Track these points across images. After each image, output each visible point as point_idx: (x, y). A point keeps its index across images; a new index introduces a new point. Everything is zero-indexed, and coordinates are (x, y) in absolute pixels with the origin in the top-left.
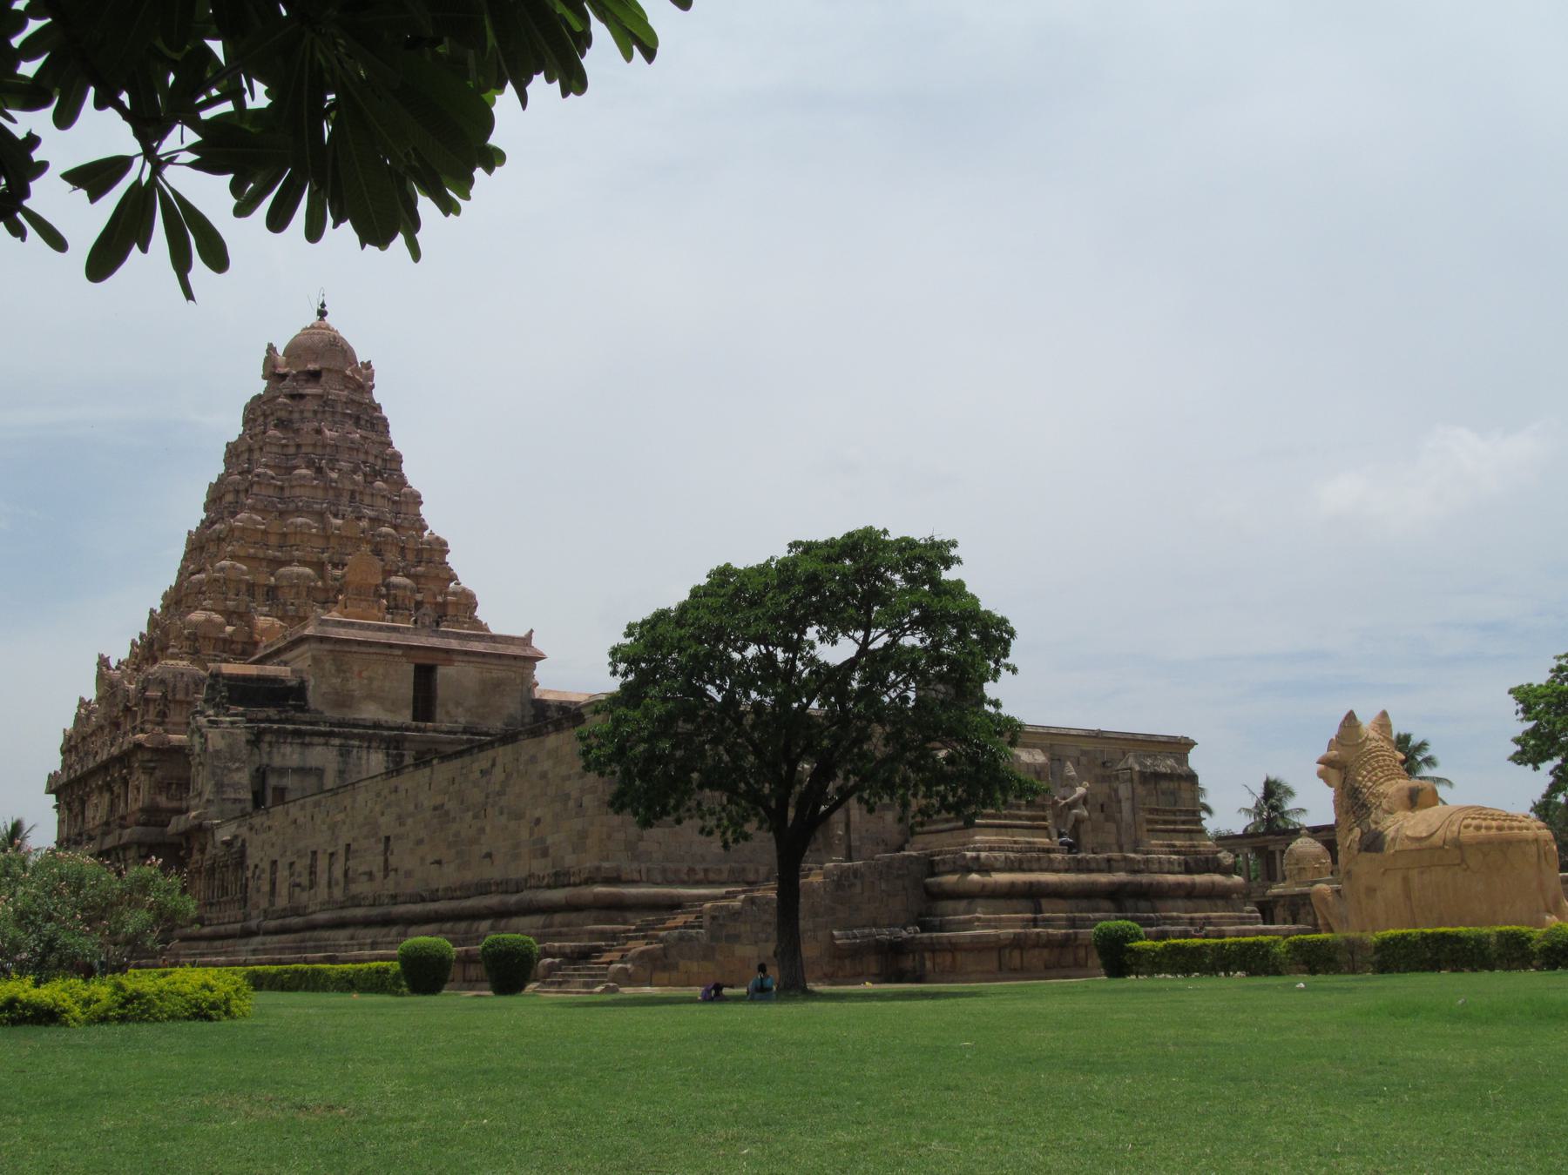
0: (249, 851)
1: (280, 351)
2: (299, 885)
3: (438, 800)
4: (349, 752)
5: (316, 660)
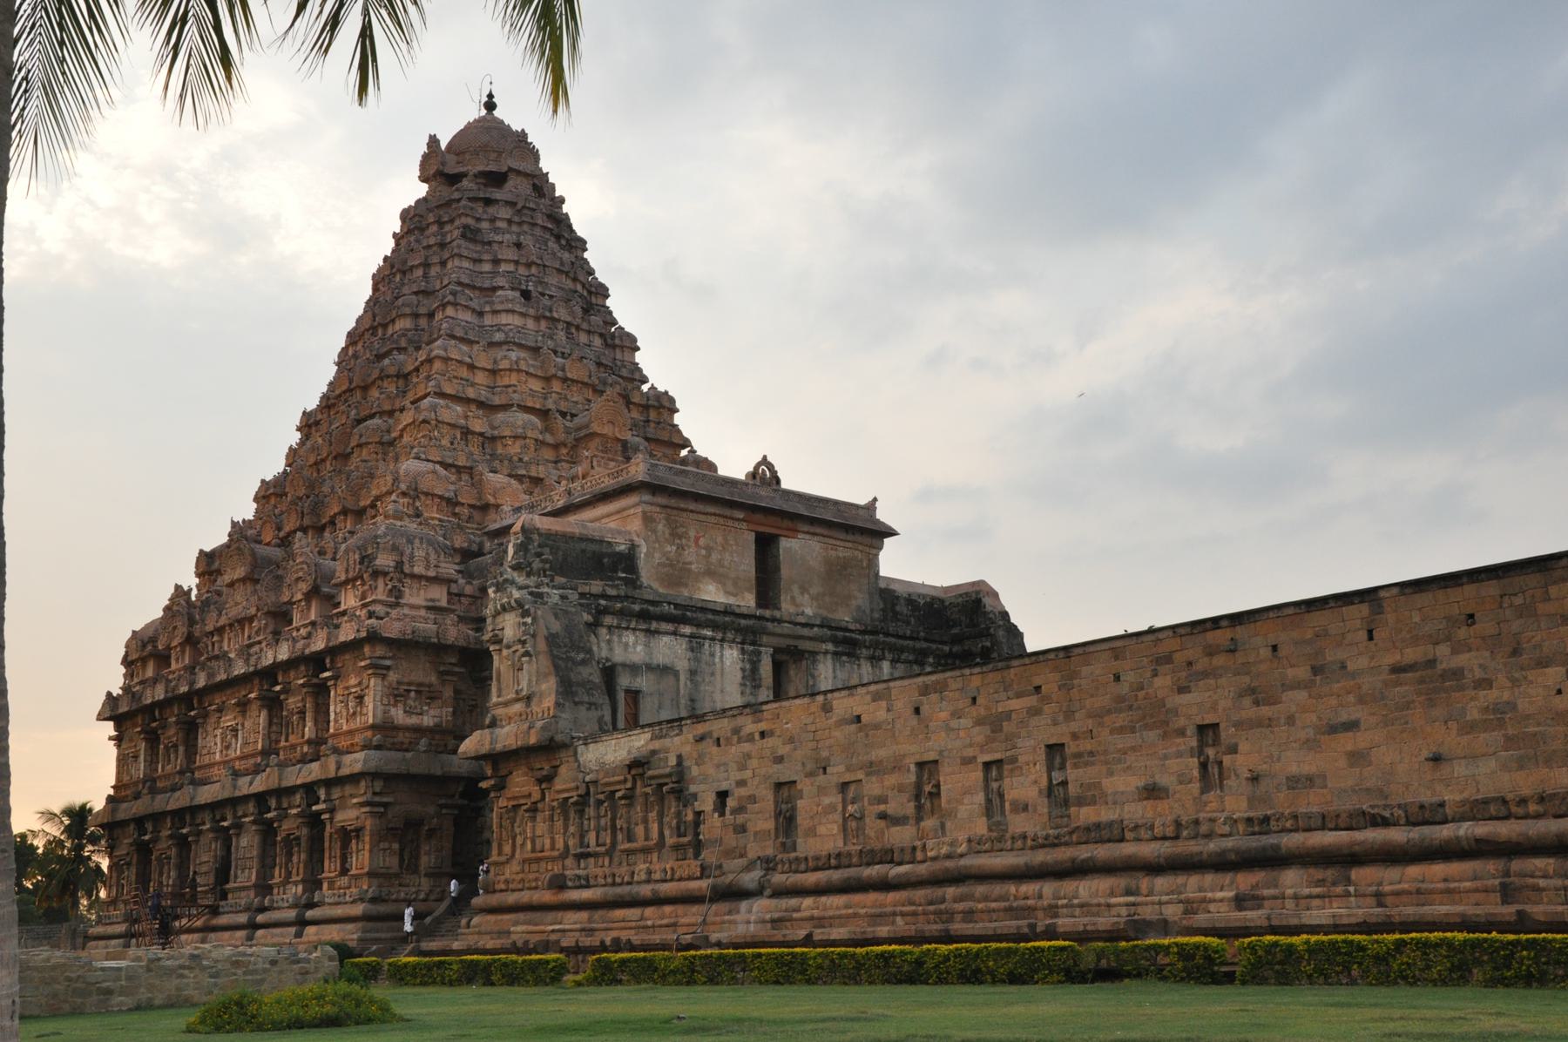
0: (695, 771)
1: (443, 146)
2: (883, 816)
3: (1411, 655)
4: (701, 646)
5: (647, 519)
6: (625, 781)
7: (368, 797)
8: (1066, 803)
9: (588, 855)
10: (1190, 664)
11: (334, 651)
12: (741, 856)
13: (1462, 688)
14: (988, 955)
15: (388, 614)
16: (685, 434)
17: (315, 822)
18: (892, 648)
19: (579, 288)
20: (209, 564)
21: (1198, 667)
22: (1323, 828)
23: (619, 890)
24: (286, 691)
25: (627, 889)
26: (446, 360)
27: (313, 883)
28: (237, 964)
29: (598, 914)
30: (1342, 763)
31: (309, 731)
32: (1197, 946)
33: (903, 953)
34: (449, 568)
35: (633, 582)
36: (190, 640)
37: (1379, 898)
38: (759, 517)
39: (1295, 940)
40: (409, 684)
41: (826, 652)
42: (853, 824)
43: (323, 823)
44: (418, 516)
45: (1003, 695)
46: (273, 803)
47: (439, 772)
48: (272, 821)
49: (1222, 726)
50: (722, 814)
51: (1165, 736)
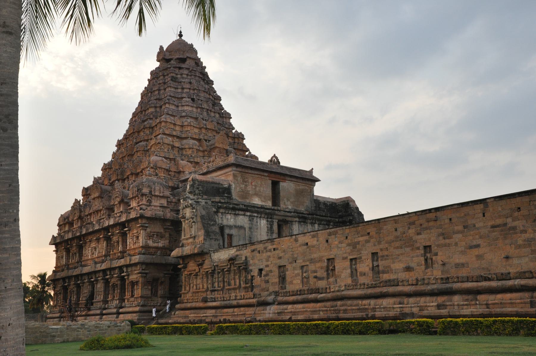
0: (251, 262)
1: (165, 49)
2: (316, 277)
3: (498, 222)
4: (253, 219)
5: (235, 176)
6: (228, 265)
7: (140, 271)
8: (378, 273)
9: (215, 290)
10: (421, 225)
11: (129, 221)
12: (267, 291)
13: (516, 233)
14: (352, 325)
15: (147, 208)
16: (247, 147)
17: (122, 279)
18: (319, 220)
19: (211, 97)
20: (86, 192)
21: (424, 226)
22: (468, 281)
23: (225, 302)
24: (112, 235)
25: (229, 302)
26: (166, 122)
27: (122, 300)
28: (97, 327)
29: (219, 310)
30: (474, 259)
31: (120, 248)
32: (424, 322)
33: (323, 324)
34: (167, 193)
35: (230, 198)
36: (80, 218)
37: (487, 305)
38: (272, 175)
39: (458, 320)
40: (154, 232)
41: (296, 221)
42: (305, 280)
43: (125, 279)
44: (157, 175)
45: (357, 236)
46: (108, 273)
47: (164, 262)
48: (108, 279)
49: (432, 246)
50: (261, 277)
51: (412, 250)
